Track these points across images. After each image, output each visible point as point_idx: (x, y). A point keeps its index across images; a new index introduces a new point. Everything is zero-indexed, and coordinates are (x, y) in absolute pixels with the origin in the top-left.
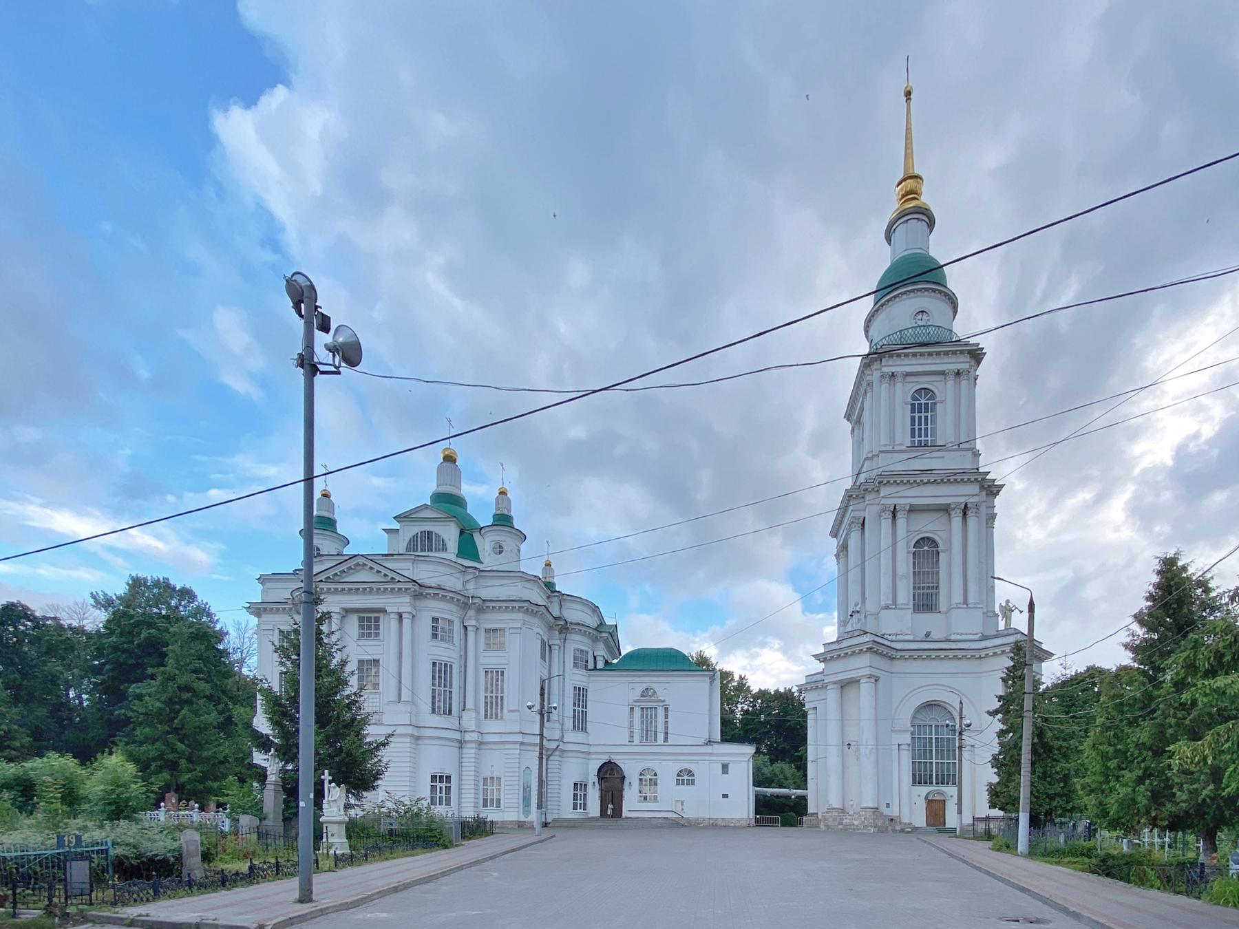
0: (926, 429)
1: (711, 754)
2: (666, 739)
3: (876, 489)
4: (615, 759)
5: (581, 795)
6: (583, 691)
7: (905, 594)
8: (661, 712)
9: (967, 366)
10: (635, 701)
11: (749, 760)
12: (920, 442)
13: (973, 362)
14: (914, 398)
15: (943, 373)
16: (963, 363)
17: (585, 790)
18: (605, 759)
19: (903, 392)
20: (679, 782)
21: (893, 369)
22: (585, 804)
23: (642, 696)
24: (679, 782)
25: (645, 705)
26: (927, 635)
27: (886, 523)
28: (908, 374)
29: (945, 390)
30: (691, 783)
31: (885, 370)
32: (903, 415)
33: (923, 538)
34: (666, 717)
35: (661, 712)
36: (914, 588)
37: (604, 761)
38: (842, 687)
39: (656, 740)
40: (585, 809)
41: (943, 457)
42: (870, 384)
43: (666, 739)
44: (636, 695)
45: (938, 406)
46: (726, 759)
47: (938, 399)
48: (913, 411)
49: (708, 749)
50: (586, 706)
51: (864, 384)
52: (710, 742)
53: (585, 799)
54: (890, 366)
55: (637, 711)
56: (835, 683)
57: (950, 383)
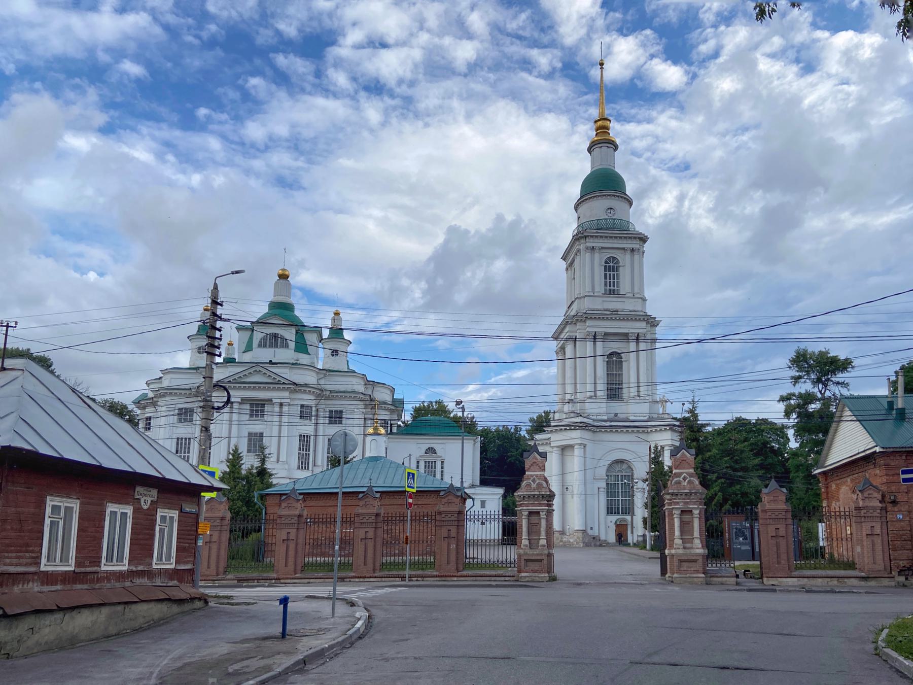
0: (614, 282)
9: (638, 246)
10: (420, 456)
12: (610, 290)
14: (606, 262)
15: (623, 249)
16: (635, 245)
19: (599, 259)
21: (594, 245)
23: (426, 453)
25: (428, 459)
28: (602, 248)
29: (625, 259)
31: (588, 244)
32: (599, 272)
38: (562, 449)
44: (422, 452)
45: (621, 269)
46: (483, 498)
48: (605, 270)
54: (590, 243)
55: (422, 465)
56: (558, 447)
57: (628, 256)
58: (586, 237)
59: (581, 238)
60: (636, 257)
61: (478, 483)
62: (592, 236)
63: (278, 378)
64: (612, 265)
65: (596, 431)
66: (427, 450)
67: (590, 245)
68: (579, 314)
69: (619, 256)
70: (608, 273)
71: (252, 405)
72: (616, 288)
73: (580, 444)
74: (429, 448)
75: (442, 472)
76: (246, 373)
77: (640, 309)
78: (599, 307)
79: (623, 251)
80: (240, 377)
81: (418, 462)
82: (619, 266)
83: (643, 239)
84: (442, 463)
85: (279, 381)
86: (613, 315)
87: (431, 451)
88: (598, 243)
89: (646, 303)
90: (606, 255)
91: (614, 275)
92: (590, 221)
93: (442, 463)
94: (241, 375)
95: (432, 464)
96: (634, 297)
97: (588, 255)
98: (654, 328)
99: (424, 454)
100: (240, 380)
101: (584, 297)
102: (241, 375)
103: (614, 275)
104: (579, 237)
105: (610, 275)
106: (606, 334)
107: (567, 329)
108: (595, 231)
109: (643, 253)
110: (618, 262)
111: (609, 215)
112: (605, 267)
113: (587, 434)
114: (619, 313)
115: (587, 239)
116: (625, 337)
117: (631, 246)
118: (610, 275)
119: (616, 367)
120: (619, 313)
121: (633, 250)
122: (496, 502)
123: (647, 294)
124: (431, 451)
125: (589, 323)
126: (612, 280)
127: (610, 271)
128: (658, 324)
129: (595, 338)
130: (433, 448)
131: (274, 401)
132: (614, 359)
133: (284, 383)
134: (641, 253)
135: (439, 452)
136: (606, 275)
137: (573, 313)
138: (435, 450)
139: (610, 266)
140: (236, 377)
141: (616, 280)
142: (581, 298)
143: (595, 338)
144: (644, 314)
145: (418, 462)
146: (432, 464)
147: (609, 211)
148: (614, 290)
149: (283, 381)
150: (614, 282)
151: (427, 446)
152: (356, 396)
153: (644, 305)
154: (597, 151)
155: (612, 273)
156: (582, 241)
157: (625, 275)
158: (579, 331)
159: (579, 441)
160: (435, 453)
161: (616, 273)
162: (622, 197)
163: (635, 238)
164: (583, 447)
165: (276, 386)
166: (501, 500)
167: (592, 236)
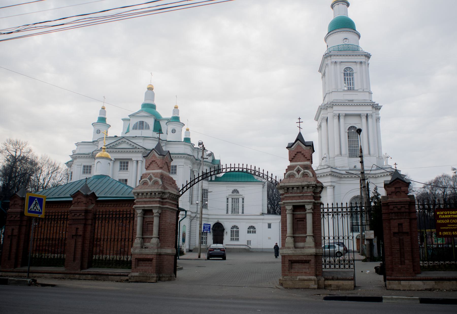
0: (350, 83)
1: (263, 219)
2: (243, 213)
3: (331, 107)
4: (221, 221)
5: (205, 238)
6: (206, 191)
7: (345, 150)
8: (241, 200)
10: (229, 195)
11: (280, 222)
13: (367, 58)
14: (345, 71)
15: (355, 62)
16: (363, 59)
17: (206, 235)
18: (216, 221)
19: (340, 69)
20: (249, 232)
22: (206, 242)
23: (232, 193)
24: (249, 232)
25: (233, 197)
26: (355, 167)
27: (336, 120)
28: (341, 62)
29: (356, 68)
30: (255, 232)
33: (351, 127)
34: (243, 202)
35: (241, 200)
36: (349, 147)
37: (216, 222)
39: (238, 213)
40: (206, 244)
41: (357, 94)
42: (327, 65)
43: (243, 213)
45: (355, 75)
46: (269, 222)
47: (354, 72)
48: (345, 75)
49: (262, 217)
50: (207, 197)
51: (325, 65)
52: (263, 214)
53: (206, 239)
54: (334, 59)
55: (230, 200)
57: (358, 66)
58: (331, 56)
59: (328, 56)
60: (364, 66)
61: (266, 212)
62: (334, 55)
63: (135, 146)
64: (348, 72)
65: (342, 177)
66: (233, 191)
67: (334, 60)
68: (328, 103)
69: (353, 66)
70: (346, 77)
71: (121, 163)
72: (352, 86)
73: (331, 186)
74: (234, 190)
75: (243, 205)
76: (117, 143)
77: (368, 99)
78: (342, 98)
79: (355, 64)
80: (114, 145)
81: (228, 199)
82: (353, 73)
83: (368, 56)
84: (243, 199)
85: (136, 147)
86: (350, 103)
87: (235, 191)
88: (339, 59)
89: (372, 96)
90: (344, 66)
91: (350, 78)
92: (334, 47)
93: (243, 199)
94: (114, 144)
95: (236, 200)
96: (363, 91)
97: (333, 66)
98: (377, 111)
99: (231, 194)
100: (114, 147)
101: (332, 92)
102: (114, 144)
103: (350, 78)
104: (327, 56)
105: (348, 78)
106: (346, 115)
107: (322, 113)
108: (337, 52)
109: (368, 64)
110: (352, 70)
111: (345, 42)
112: (344, 74)
113: (335, 179)
114: (354, 101)
115: (332, 57)
116: (359, 116)
117: (360, 60)
118: (348, 78)
119: (354, 136)
120: (354, 101)
121: (361, 63)
122: (278, 223)
123: (372, 90)
124: (235, 191)
125: (335, 108)
126: (349, 82)
127: (347, 76)
128: (380, 108)
129: (339, 117)
130: (236, 190)
131: (133, 159)
132: (353, 130)
133: (138, 148)
134: (367, 65)
135: (241, 193)
136: (345, 78)
137: (326, 103)
138: (238, 191)
139: (347, 73)
140: (111, 145)
141: (351, 82)
142: (329, 93)
143: (339, 117)
144: (370, 101)
145: (228, 199)
146: (236, 200)
147: (345, 40)
148: (351, 88)
149: (138, 147)
150: (350, 83)
151: (233, 189)
152: (185, 157)
153: (371, 97)
154: (336, 7)
155: (349, 77)
156: (329, 58)
157: (357, 77)
158: (329, 113)
159: (330, 184)
160: (239, 193)
161: (351, 77)
162: (353, 32)
163: (362, 55)
164: (332, 187)
165: (134, 150)
166: (281, 223)
167: (334, 55)
